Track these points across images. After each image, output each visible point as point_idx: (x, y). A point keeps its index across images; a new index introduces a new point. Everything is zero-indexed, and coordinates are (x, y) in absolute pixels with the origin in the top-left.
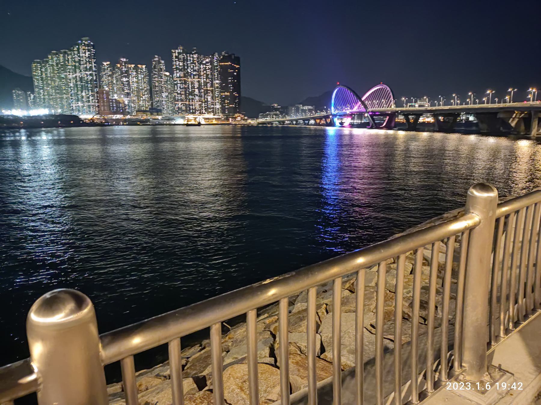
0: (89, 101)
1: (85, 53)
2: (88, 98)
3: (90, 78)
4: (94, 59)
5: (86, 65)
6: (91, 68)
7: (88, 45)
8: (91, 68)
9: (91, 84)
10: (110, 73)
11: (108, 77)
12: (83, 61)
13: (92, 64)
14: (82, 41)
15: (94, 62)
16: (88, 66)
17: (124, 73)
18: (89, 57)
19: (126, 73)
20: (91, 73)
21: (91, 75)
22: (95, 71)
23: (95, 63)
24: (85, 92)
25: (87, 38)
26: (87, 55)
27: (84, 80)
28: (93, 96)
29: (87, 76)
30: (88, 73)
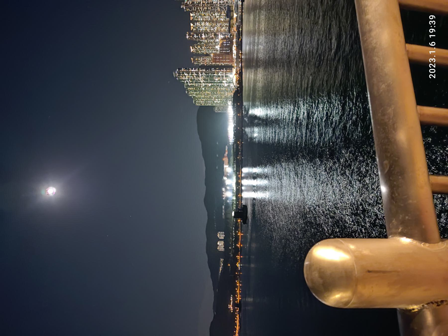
0: (223, 76)
1: (185, 76)
2: (219, 76)
3: (204, 74)
4: (189, 69)
5: (195, 76)
6: (197, 73)
7: (179, 73)
8: (197, 73)
9: (208, 74)
10: (199, 47)
11: (202, 49)
12: (191, 78)
13: (193, 72)
14: (176, 77)
15: (192, 70)
16: (195, 74)
17: (198, 37)
18: (188, 74)
19: (198, 35)
20: (200, 73)
21: (201, 74)
22: (199, 69)
23: (192, 69)
24: (215, 78)
25: (174, 73)
26: (187, 75)
27: (206, 78)
28: (218, 73)
29: (203, 76)
30: (200, 75)
